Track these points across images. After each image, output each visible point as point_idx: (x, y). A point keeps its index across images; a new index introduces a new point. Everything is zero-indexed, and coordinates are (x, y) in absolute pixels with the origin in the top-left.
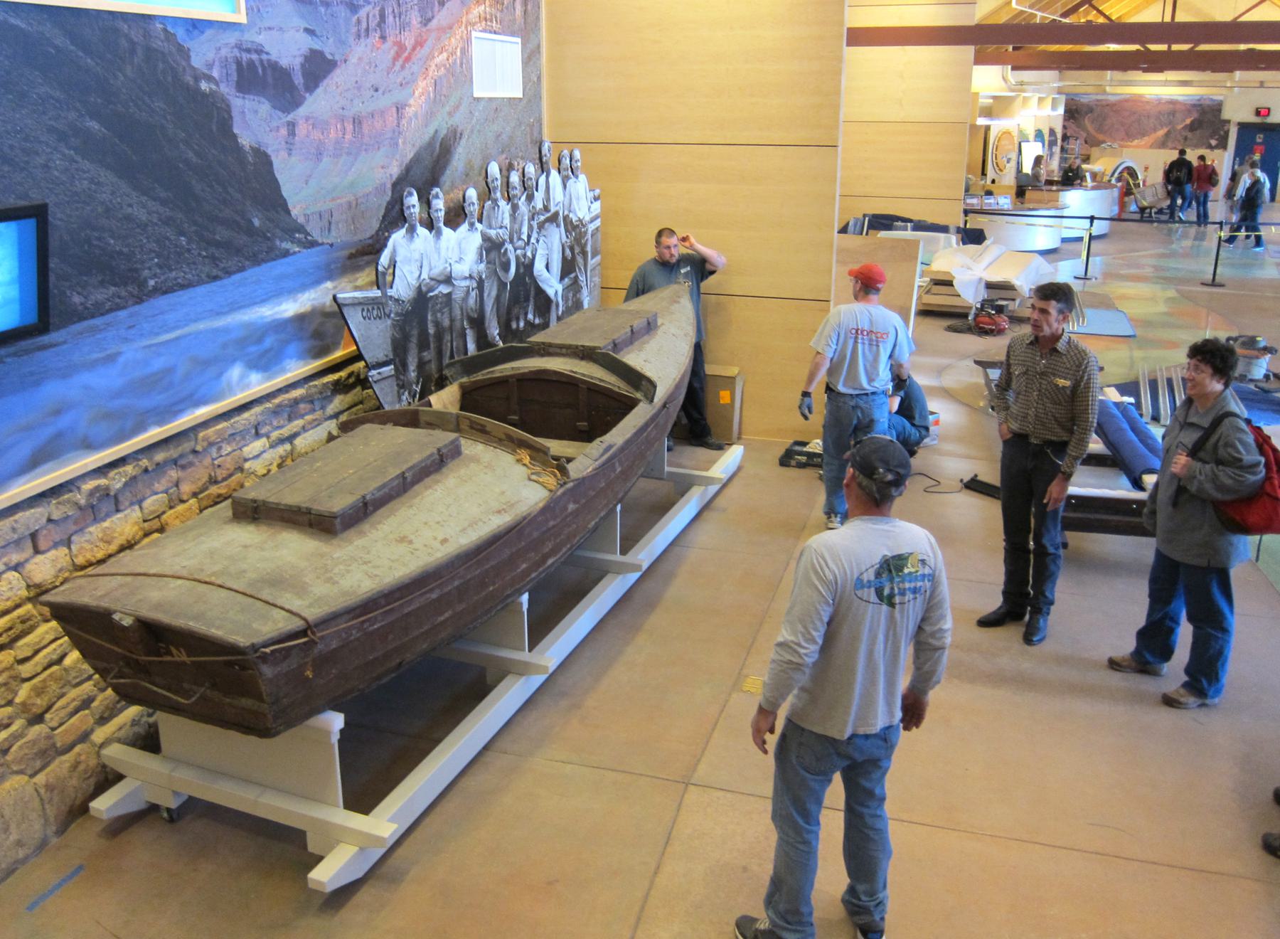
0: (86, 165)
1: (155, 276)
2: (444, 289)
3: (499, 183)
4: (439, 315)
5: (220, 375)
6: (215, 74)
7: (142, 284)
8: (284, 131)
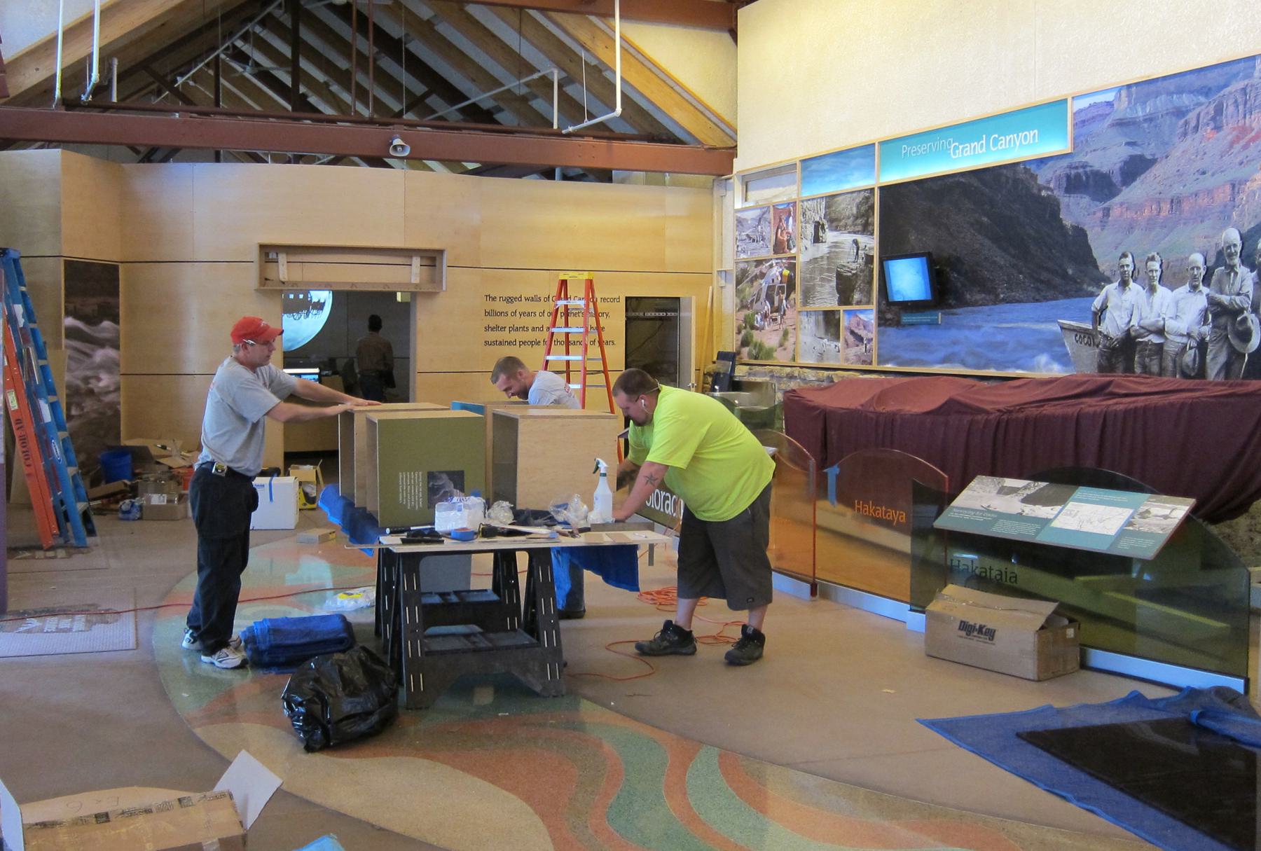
0: (979, 237)
2: (1155, 339)
3: (1239, 249)
4: (1147, 360)
5: (1034, 356)
6: (1052, 186)
8: (1100, 214)
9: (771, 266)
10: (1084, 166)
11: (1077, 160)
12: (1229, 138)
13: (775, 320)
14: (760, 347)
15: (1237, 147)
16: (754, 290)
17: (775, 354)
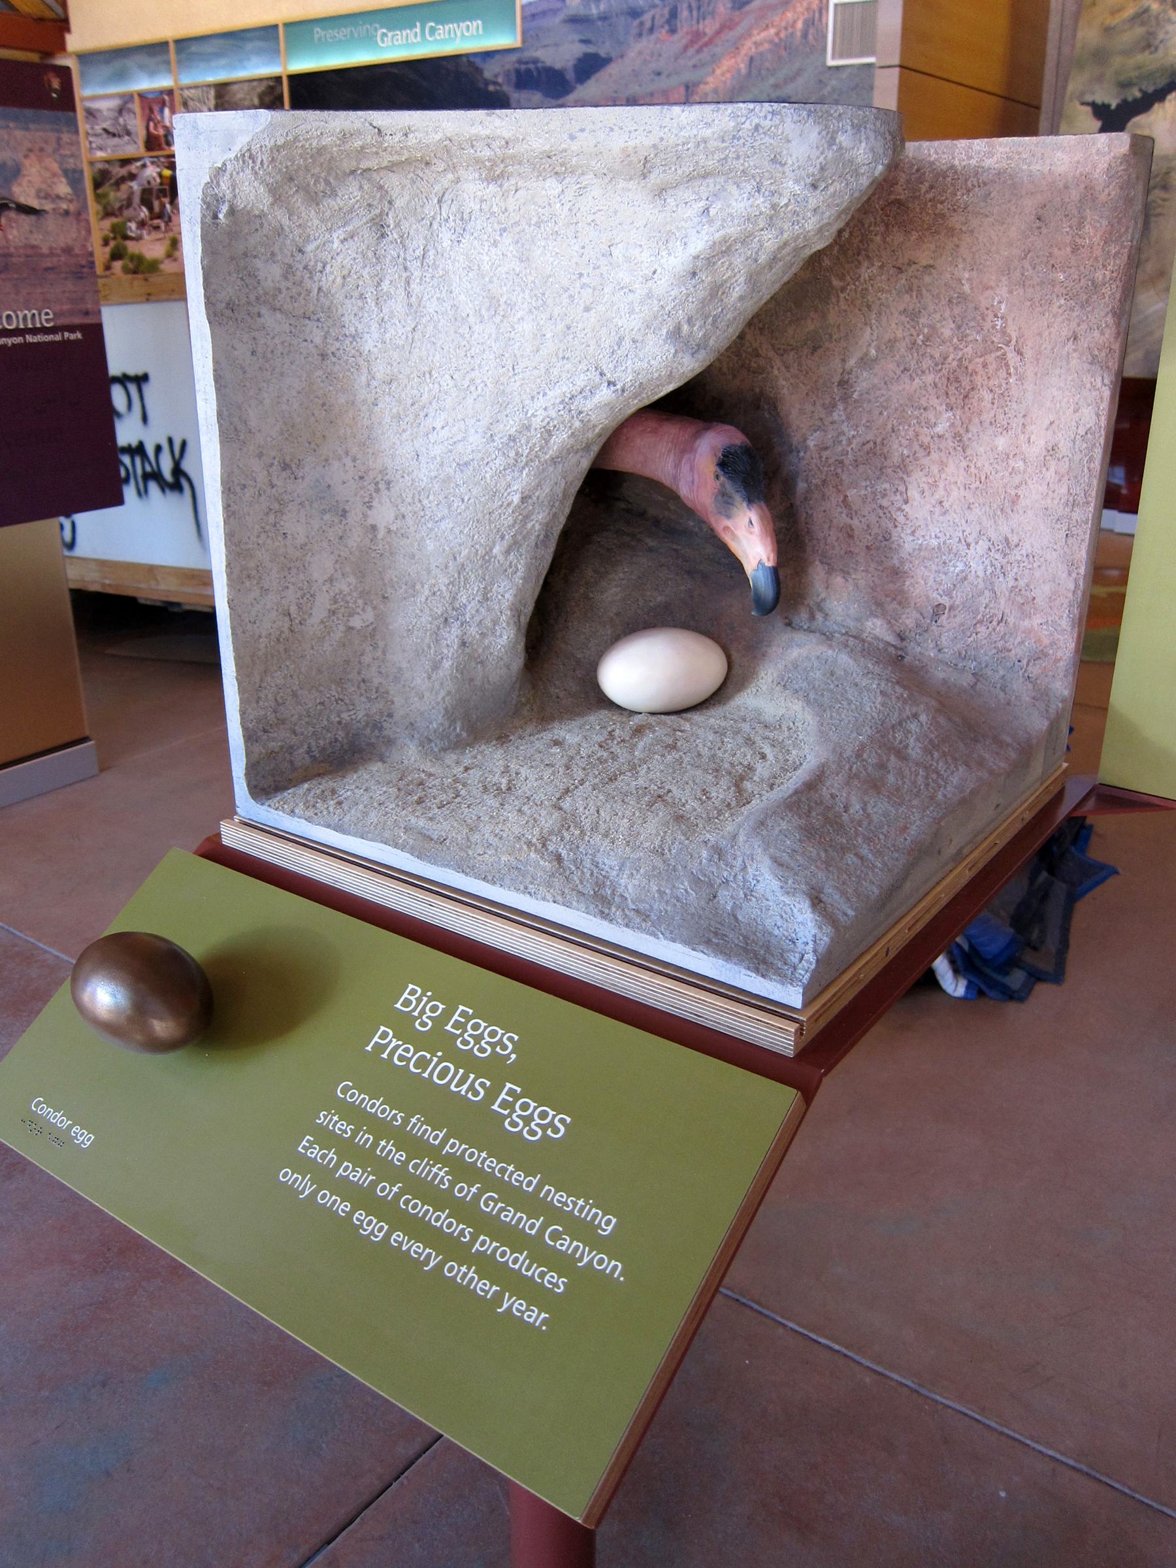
6: (500, 80)
9: (144, 166)
10: (535, 61)
11: (527, 55)
12: (684, 41)
13: (157, 228)
14: (139, 260)
15: (691, 51)
16: (122, 193)
17: (162, 267)
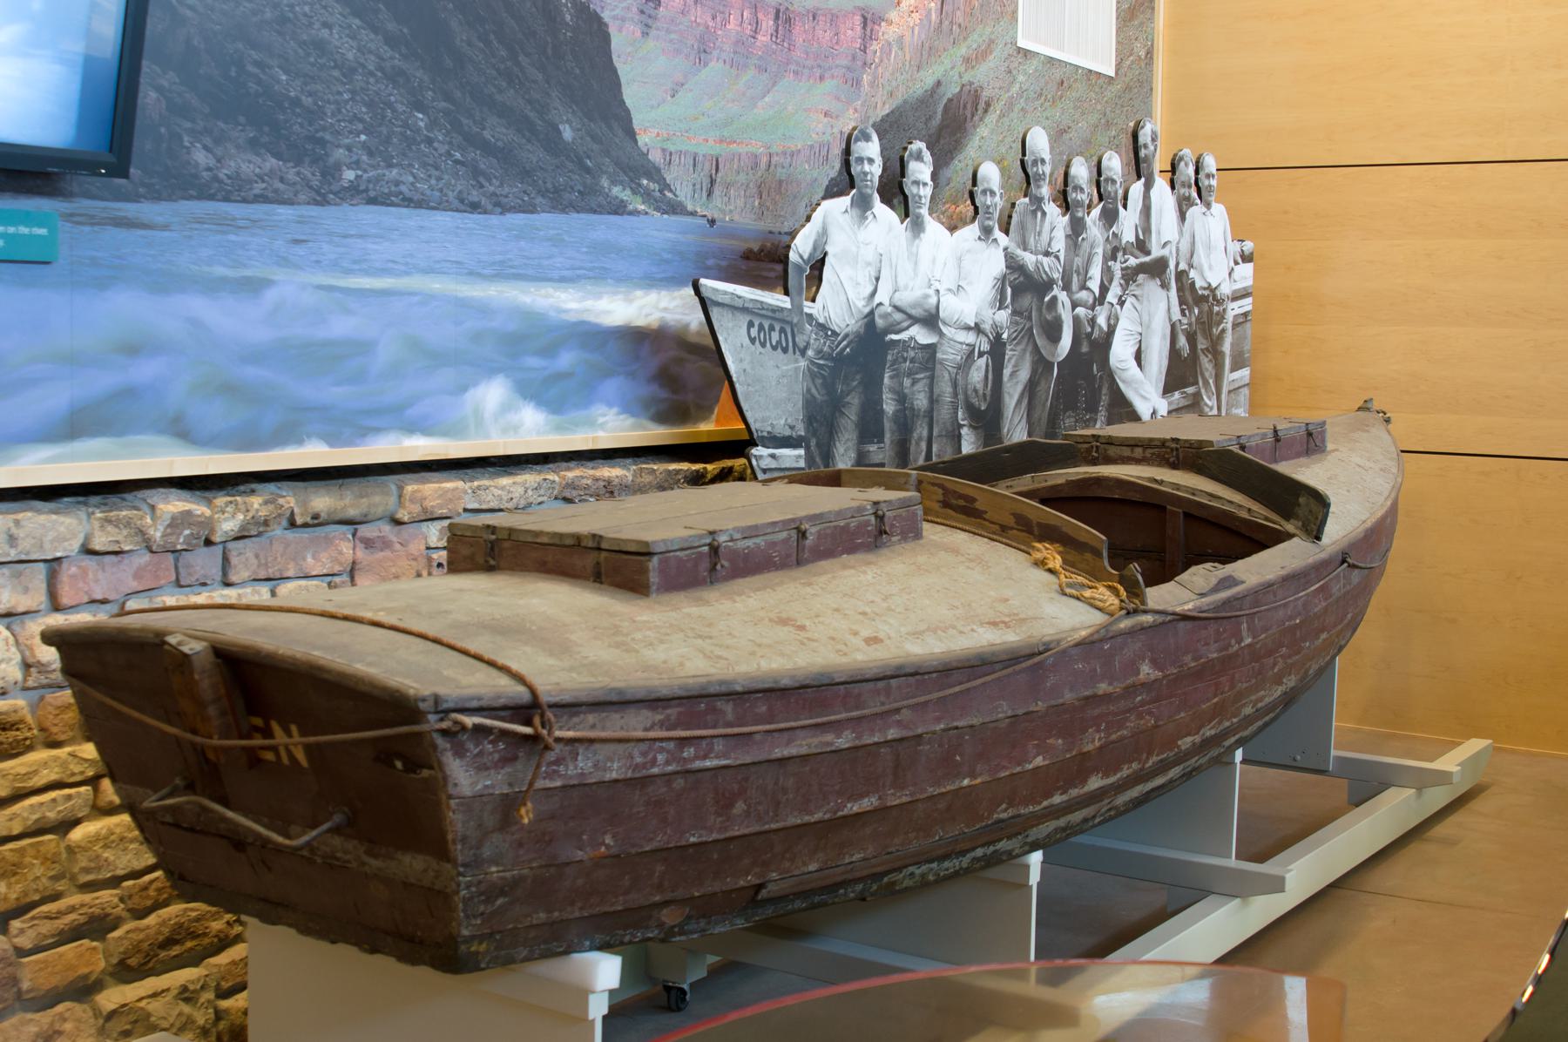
1: (356, 165)
2: (921, 335)
3: (1047, 169)
4: (907, 382)
5: (464, 389)
7: (330, 173)
